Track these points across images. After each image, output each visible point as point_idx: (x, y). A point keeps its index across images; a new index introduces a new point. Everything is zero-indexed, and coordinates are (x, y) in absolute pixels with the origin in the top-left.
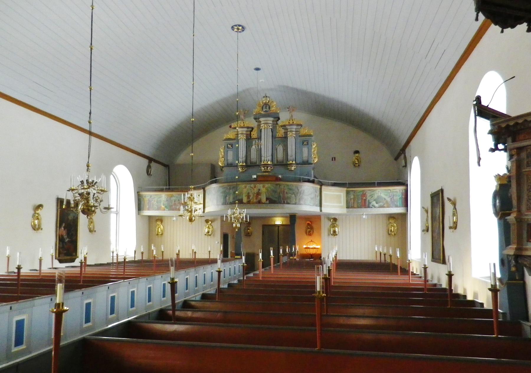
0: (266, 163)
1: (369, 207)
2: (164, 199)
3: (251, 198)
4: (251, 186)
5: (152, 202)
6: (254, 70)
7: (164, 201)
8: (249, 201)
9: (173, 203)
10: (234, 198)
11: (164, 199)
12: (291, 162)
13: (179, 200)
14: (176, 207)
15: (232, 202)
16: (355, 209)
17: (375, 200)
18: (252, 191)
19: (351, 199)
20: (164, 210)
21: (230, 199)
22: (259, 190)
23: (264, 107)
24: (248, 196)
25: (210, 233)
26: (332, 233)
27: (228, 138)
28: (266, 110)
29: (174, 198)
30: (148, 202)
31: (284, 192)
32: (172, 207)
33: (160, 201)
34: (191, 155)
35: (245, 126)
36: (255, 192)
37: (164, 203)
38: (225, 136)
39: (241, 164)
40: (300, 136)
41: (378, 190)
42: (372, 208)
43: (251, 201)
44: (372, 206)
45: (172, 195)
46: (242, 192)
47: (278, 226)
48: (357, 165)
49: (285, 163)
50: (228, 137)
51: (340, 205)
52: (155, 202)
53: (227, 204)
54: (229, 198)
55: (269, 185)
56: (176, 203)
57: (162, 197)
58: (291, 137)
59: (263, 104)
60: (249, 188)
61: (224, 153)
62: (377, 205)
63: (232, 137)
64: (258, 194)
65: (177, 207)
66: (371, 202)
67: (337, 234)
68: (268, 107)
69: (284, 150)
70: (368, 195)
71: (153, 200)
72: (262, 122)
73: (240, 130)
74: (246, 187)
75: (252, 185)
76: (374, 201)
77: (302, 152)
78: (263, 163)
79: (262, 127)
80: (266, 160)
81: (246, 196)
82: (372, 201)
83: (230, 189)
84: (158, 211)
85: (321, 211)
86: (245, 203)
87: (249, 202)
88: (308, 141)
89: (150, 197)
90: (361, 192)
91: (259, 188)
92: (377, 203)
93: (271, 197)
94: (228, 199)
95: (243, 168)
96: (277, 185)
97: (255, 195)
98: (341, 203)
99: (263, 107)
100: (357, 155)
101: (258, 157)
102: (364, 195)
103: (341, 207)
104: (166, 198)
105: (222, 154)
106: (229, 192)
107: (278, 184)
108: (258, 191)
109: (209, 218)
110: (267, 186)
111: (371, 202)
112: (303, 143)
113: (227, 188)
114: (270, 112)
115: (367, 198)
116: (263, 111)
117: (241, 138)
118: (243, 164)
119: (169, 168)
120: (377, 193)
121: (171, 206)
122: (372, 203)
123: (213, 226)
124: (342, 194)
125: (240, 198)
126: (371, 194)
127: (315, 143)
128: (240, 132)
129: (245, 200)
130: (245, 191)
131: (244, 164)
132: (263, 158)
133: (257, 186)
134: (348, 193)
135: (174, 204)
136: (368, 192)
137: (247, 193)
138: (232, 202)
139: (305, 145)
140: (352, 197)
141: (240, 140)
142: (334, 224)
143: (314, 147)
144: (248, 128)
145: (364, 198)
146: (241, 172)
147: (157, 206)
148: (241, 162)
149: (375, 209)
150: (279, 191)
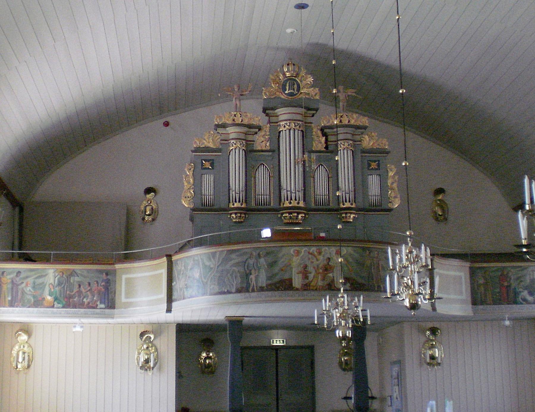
0: (294, 204)
1: (515, 302)
2: (52, 281)
3: (311, 276)
4: (311, 252)
5: (20, 287)
6: (309, 5)
7: (51, 284)
8: (306, 285)
9: (76, 290)
10: (269, 278)
11: (52, 281)
12: (347, 205)
13: (89, 284)
14: (83, 299)
15: (264, 285)
16: (488, 306)
17: (526, 288)
18: (312, 262)
19: (479, 286)
20: (53, 307)
21: (260, 280)
22: (329, 259)
23: (288, 85)
24: (305, 274)
25: (152, 364)
26: (428, 360)
27: (203, 146)
28: (292, 91)
29: (77, 279)
30: (10, 286)
31: (378, 267)
32: (71, 300)
33: (42, 286)
34: (404, 164)
35: (246, 122)
36: (320, 266)
37: (52, 290)
38: (195, 142)
39: (237, 205)
40: (364, 151)
41: (532, 267)
42: (521, 304)
43: (312, 284)
44: (521, 301)
45: (74, 270)
46: (290, 265)
47: (277, 349)
48: (442, 218)
49: (332, 205)
50: (204, 143)
51: (459, 297)
52: (29, 288)
53: (250, 290)
54: (257, 277)
55: (350, 249)
56: (83, 291)
57: (46, 275)
58: (345, 151)
59: (286, 79)
60: (307, 254)
61: (194, 180)
62: (530, 298)
63: (211, 145)
64: (327, 269)
65: (85, 300)
66: (520, 292)
67: (439, 361)
68: (296, 86)
69: (331, 179)
70: (512, 278)
71: (23, 283)
72: (281, 118)
73: (230, 130)
74: (298, 253)
75: (313, 249)
76: (526, 289)
77: (365, 185)
78: (287, 204)
79: (285, 126)
80: (293, 198)
81: (300, 272)
82: (521, 290)
83: (259, 256)
84: (36, 309)
85: (434, 309)
86: (297, 289)
87: (306, 287)
88: (379, 161)
89: (15, 274)
90: (497, 271)
91: (328, 256)
92: (531, 294)
93: (353, 276)
94: (254, 279)
95: (241, 213)
96: (364, 249)
97: (321, 271)
98: (461, 293)
99: (286, 85)
100: (440, 197)
101: (272, 191)
102: (504, 277)
103: (463, 302)
104: (57, 278)
105: (189, 182)
106: (257, 263)
107: (368, 248)
108: (325, 262)
109: (149, 328)
110: (344, 251)
111: (520, 292)
112: (369, 165)
113: (251, 254)
114: (300, 97)
115: (511, 284)
116: (286, 94)
117: (235, 149)
118: (242, 204)
119: (21, 210)
120: (530, 274)
121: (71, 297)
122: (522, 294)
123: (158, 347)
124: (462, 274)
125: (286, 277)
126: (520, 275)
127: (393, 167)
128: (232, 136)
129: (297, 282)
130: (296, 261)
131: (243, 206)
132: (284, 193)
133: (323, 250)
134: (473, 272)
135: (77, 292)
136: (512, 270)
137: (302, 266)
138: (264, 285)
139: (372, 169)
140: (481, 281)
141: (233, 153)
142: (432, 340)
143: (391, 174)
144: (250, 126)
145: (506, 284)
146: (235, 222)
147: (34, 297)
148: (237, 200)
149: (528, 306)
150: (368, 263)
